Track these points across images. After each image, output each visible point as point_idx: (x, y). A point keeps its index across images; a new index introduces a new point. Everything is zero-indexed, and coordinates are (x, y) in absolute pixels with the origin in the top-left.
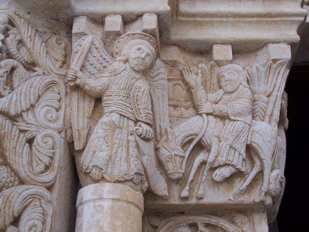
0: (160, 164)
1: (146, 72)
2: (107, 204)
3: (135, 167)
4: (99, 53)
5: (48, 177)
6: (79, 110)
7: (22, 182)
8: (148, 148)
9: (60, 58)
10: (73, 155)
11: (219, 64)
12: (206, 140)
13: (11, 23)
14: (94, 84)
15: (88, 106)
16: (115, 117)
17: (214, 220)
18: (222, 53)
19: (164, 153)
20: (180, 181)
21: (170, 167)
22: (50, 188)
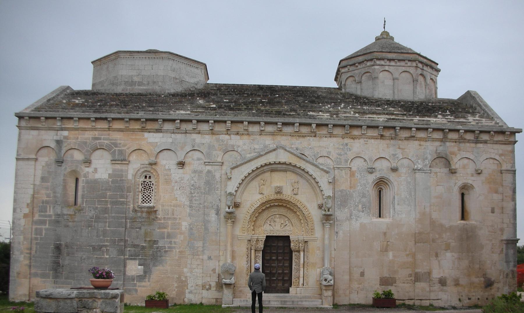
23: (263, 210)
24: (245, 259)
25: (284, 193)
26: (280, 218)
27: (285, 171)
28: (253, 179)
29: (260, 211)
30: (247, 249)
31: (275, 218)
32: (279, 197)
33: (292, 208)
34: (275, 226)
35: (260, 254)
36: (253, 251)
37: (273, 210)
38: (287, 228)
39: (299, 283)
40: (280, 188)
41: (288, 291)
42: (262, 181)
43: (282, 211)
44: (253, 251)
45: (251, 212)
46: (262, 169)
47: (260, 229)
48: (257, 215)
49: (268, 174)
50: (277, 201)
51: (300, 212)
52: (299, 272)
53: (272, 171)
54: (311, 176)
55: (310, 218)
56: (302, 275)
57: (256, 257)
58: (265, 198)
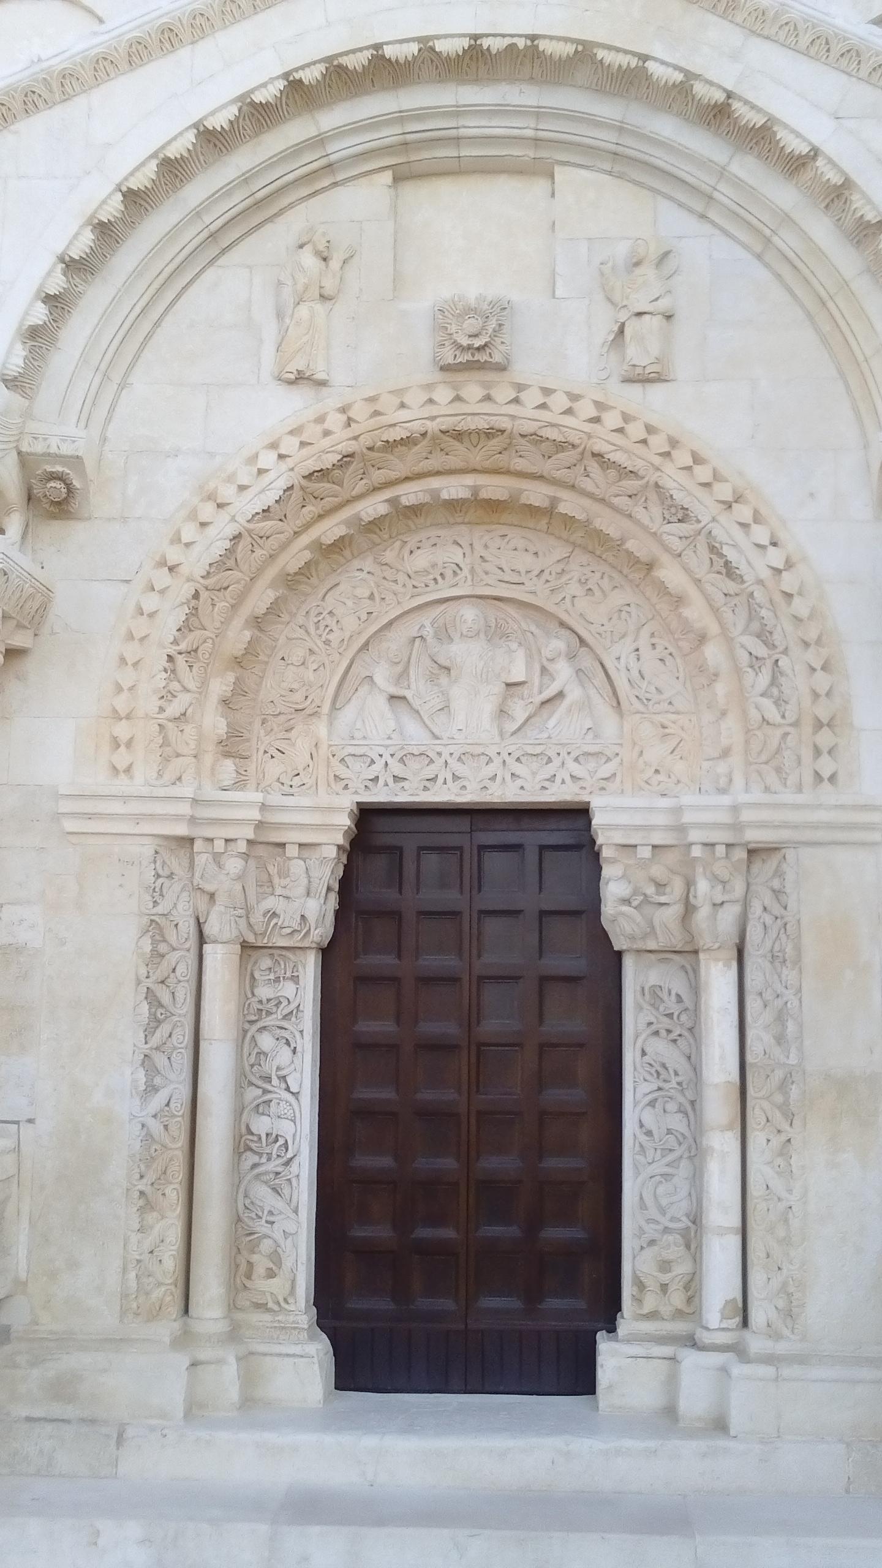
0: (250, 925)
1: (240, 878)
2: (219, 956)
3: (235, 933)
4: (212, 867)
5: (187, 946)
6: (202, 903)
7: (174, 949)
8: (243, 922)
9: (187, 865)
10: (199, 925)
11: (289, 859)
12: (277, 912)
13: (157, 853)
14: (209, 887)
15: (206, 898)
16: (222, 909)
17: (284, 953)
18: (292, 851)
19: (252, 920)
20: (264, 934)
21: (256, 927)
22: (188, 950)
23: (334, 551)
24: (125, 1033)
25: (528, 367)
26: (496, 634)
27: (532, 161)
28: (216, 243)
29: (295, 558)
30: (155, 928)
31: (444, 634)
32: (473, 403)
33: (608, 523)
34: (445, 708)
35: (303, 990)
36: (220, 961)
37: (421, 560)
38: (562, 726)
39: (693, 1287)
40: (497, 314)
41: (578, 1377)
42: (308, 259)
43: (513, 558)
44: (220, 961)
45: (195, 564)
46: (295, 131)
47: (301, 747)
48: (262, 598)
49: (359, 205)
50: (460, 455)
51: (699, 560)
52: (697, 1178)
53: (411, 164)
54: (795, 165)
55: (800, 607)
56: (722, 1213)
57: (251, 1018)
58: (335, 421)
